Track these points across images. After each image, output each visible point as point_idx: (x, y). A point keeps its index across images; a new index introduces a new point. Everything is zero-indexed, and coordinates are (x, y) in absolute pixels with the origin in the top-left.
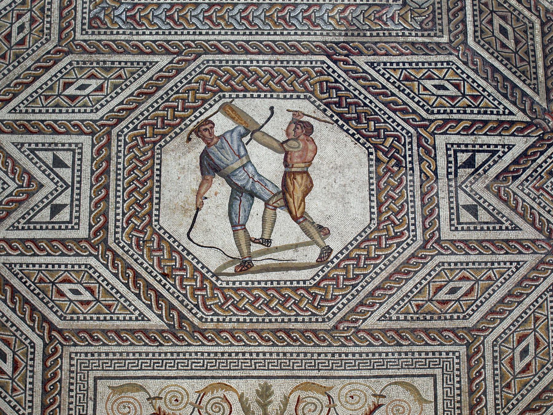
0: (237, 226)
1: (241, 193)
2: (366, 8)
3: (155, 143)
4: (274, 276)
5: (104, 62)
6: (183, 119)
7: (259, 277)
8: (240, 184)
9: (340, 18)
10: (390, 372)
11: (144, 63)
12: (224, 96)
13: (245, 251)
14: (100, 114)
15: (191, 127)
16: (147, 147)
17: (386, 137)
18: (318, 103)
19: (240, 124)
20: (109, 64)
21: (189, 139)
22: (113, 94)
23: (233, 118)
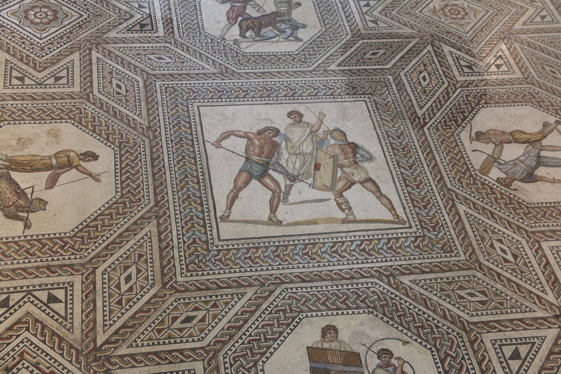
1: (540, 162)
2: (380, 111)
3: (527, 207)
5: (477, 241)
6: (502, 194)
8: (535, 163)
9: (392, 122)
11: (468, 218)
12: (476, 174)
14: (520, 239)
15: (506, 189)
16: (532, 211)
17: (468, 100)
18: (459, 130)
19: (492, 166)
20: (478, 238)
21: (515, 190)
22: (501, 233)
23: (490, 169)
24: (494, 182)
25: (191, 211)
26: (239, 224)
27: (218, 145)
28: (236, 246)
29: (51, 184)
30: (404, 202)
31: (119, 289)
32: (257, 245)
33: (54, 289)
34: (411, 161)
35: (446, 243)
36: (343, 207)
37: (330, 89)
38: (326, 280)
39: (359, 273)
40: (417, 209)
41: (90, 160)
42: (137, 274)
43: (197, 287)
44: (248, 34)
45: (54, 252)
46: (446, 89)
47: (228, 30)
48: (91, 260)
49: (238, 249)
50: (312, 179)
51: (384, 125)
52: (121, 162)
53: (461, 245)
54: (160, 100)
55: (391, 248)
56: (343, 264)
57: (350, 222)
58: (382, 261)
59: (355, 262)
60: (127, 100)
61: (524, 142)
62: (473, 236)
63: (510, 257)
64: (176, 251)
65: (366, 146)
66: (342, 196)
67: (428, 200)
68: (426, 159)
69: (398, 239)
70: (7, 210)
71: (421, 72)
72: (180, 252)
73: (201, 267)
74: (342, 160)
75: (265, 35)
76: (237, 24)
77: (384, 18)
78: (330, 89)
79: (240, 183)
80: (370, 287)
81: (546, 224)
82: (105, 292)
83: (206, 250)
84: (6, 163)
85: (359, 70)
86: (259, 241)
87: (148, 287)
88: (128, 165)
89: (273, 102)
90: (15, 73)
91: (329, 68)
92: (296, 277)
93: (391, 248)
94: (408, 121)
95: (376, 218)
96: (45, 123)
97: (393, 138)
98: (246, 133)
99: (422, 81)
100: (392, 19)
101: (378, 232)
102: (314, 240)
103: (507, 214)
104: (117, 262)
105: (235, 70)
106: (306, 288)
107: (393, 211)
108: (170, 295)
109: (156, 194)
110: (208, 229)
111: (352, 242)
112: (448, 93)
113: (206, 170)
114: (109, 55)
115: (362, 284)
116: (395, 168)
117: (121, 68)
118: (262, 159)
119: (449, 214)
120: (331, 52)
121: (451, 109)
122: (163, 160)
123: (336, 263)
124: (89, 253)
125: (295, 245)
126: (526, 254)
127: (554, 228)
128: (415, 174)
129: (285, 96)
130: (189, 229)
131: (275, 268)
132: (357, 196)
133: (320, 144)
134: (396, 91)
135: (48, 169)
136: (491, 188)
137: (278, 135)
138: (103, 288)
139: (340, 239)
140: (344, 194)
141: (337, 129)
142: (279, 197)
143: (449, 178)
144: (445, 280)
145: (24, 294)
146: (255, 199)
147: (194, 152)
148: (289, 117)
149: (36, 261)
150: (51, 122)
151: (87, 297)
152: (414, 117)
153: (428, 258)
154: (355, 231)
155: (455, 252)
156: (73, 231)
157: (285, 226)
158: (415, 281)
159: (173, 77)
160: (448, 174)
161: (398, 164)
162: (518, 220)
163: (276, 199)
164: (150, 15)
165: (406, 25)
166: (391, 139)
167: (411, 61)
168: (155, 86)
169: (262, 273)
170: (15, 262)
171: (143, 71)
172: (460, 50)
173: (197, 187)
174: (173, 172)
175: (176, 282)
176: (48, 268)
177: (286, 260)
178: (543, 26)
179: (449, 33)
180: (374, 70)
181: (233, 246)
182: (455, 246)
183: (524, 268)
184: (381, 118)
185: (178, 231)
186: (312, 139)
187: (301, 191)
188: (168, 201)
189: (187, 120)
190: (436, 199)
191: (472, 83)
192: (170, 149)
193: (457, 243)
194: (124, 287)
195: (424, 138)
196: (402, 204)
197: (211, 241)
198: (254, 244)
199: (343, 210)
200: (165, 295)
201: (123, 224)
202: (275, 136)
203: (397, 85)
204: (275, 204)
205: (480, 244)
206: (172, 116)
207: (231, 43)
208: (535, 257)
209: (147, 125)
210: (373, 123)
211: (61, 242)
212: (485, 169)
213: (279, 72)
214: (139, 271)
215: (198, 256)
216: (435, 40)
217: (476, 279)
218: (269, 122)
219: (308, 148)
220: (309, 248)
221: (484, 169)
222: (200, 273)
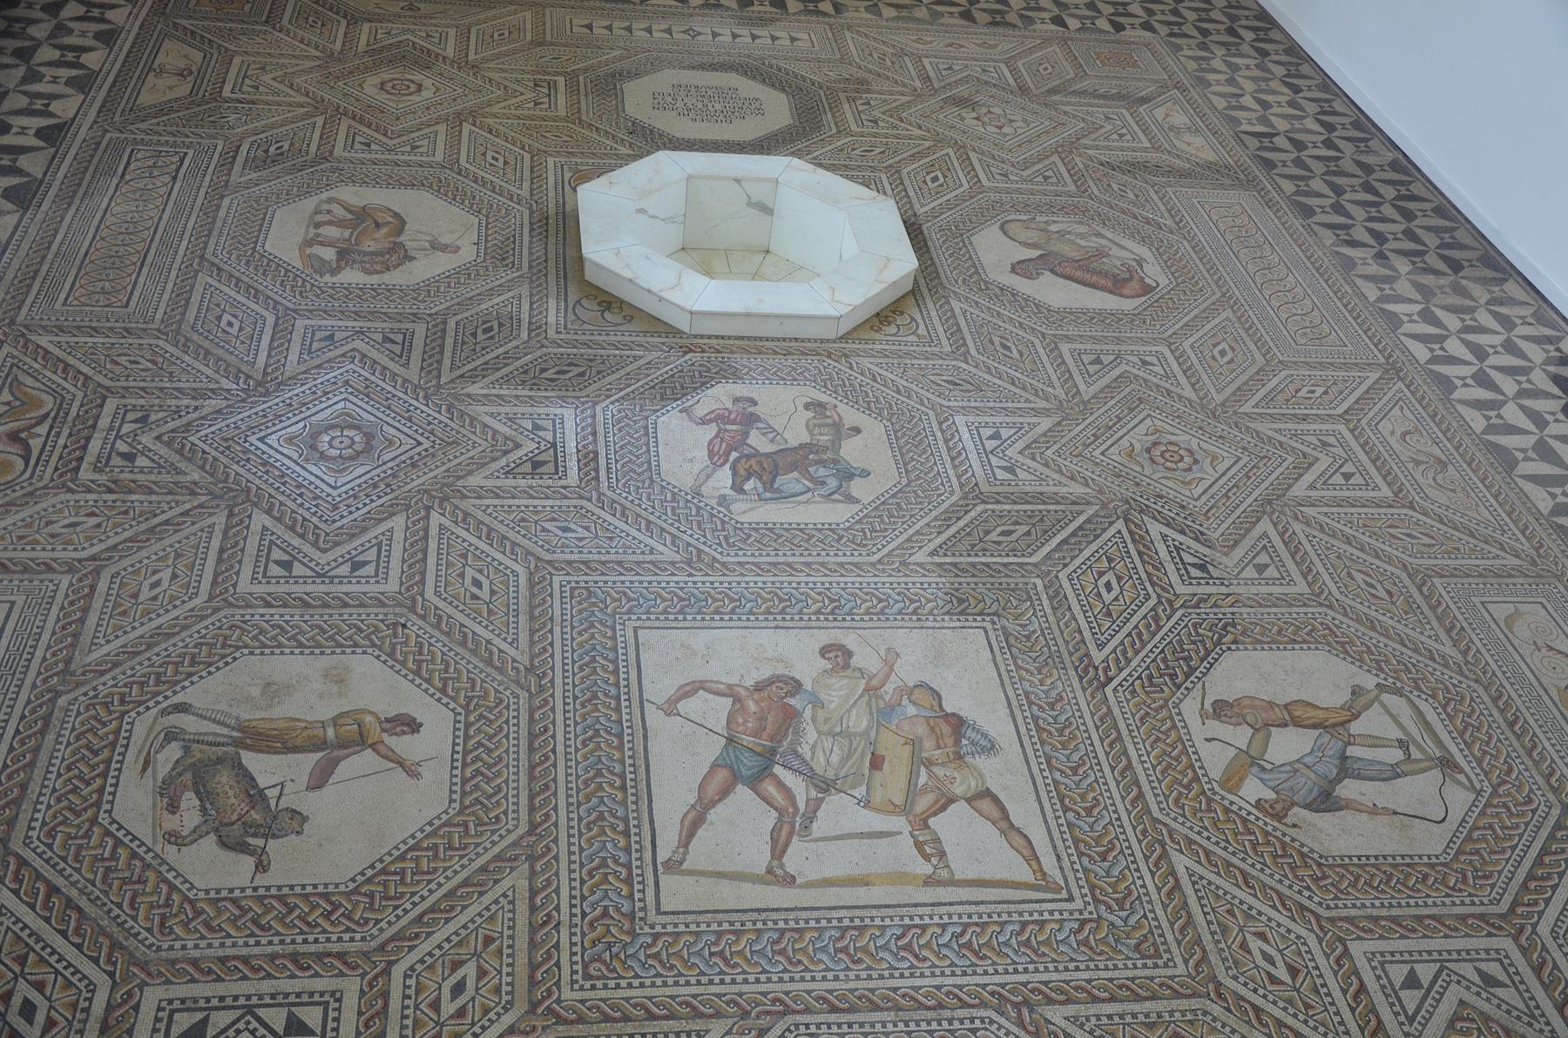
0: (1395, 773)
1: (1346, 768)
3: (1320, 865)
4: (1444, 736)
5: (1213, 934)
6: (1267, 834)
7: (1454, 750)
8: (1335, 771)
9: (1040, 673)
10: (1502, 637)
11: (1194, 883)
13: (1427, 764)
14: (1304, 933)
17: (1198, 634)
20: (1214, 927)
21: (1294, 826)
22: (1264, 918)
23: (1242, 780)
24: (1249, 808)
25: (604, 848)
26: (703, 880)
27: (670, 708)
28: (693, 928)
29: (320, 779)
30: (1059, 843)
31: (437, 1010)
32: (738, 926)
33: (302, 1004)
34: (1076, 757)
35: (1145, 936)
36: (929, 851)
37: (912, 601)
38: (882, 1009)
39: (956, 996)
40: (1085, 860)
41: (404, 733)
42: (479, 978)
43: (603, 1013)
44: (746, 487)
45: (309, 924)
46: (1152, 609)
47: (709, 476)
48: (382, 947)
49: (697, 934)
50: (864, 788)
51: (1021, 679)
52: (467, 737)
53: (1179, 943)
54: (557, 612)
55: (1027, 944)
56: (922, 975)
57: (940, 883)
58: (1007, 972)
59: (948, 971)
60: (490, 612)
61: (1314, 726)
62: (1204, 923)
63: (1282, 973)
64: (564, 932)
65: (982, 723)
66: (927, 827)
67: (1110, 842)
68: (1107, 754)
69: (1042, 924)
70: (224, 831)
71: (1101, 574)
72: (572, 934)
73: (614, 970)
74: (929, 749)
75: (784, 488)
76: (728, 466)
77: (1029, 462)
78: (912, 601)
79: (711, 790)
80: (978, 1029)
81: (1358, 903)
82: (407, 1017)
83: (628, 933)
84: (235, 734)
85: (973, 565)
86: (743, 917)
87: (499, 1009)
88: (480, 744)
89: (791, 624)
90: (277, 554)
91: (912, 559)
92: (817, 999)
93: (1027, 944)
94: (1072, 673)
95: (998, 877)
96: (322, 653)
97: (1040, 707)
98: (730, 687)
99: (1103, 591)
100: (1046, 465)
101: (1000, 907)
102: (862, 920)
103: (1277, 877)
104: (437, 952)
105: (718, 556)
106: (839, 1025)
107: (1033, 863)
108: (544, 1028)
109: (532, 810)
110: (637, 887)
111: (944, 927)
112: (1156, 618)
113: (641, 763)
114: (464, 520)
115: (961, 1021)
116: (1042, 771)
117: (486, 548)
118: (762, 743)
119: (1153, 874)
120: (917, 527)
121: (1162, 651)
122: (553, 737)
123: (907, 973)
124: (381, 930)
125: (821, 930)
126: (1317, 968)
127: (1375, 912)
128: (1085, 784)
129: (818, 612)
130: (597, 886)
131: (775, 978)
132: (960, 830)
133: (884, 714)
134: (1048, 610)
135: (317, 749)
136: (1244, 821)
137: (797, 692)
138: (405, 1007)
139: (917, 921)
140: (931, 821)
141: (921, 685)
142: (793, 825)
143: (1156, 795)
144: (1141, 1018)
145: (239, 1013)
146: (742, 826)
147: (620, 722)
148: (823, 656)
149: (270, 943)
150: (333, 653)
151: (367, 1026)
152: (1085, 666)
153: (1107, 969)
154: (951, 904)
155: (1166, 956)
156: (353, 880)
157: (801, 886)
158: (1076, 1018)
159: (588, 567)
160: (1153, 788)
161: (1049, 762)
162: (1300, 892)
163: (786, 828)
164: (554, 445)
165: (1072, 479)
166: (1035, 708)
167: (1081, 551)
168: (551, 584)
169: (745, 988)
170: (229, 942)
171: (529, 553)
172: (1182, 532)
173: (620, 796)
174: (573, 763)
175: (558, 1001)
176: (294, 958)
177: (800, 962)
178: (1348, 493)
179: (1162, 497)
180: (1005, 565)
181: (687, 926)
182: (1165, 943)
183: (1313, 999)
184: (1016, 664)
185: (571, 888)
186: (869, 704)
187: (840, 812)
188: (556, 824)
189: (611, 656)
190: (1127, 840)
191: (1206, 601)
192: (571, 715)
193: (1170, 937)
194: (448, 1008)
195: (1105, 709)
196: (1055, 847)
197: (641, 914)
198: (732, 924)
199: (927, 858)
200: (534, 1028)
201: (457, 871)
202: (793, 695)
203: (1051, 599)
204: (782, 840)
205: (1219, 942)
206: (581, 645)
207: (713, 502)
208: (1335, 973)
209: (527, 663)
210: (1000, 675)
211: (326, 904)
212: (1232, 780)
213: (808, 564)
214: (482, 973)
215: (610, 946)
216: (1132, 512)
217: (1208, 1019)
218: (779, 665)
219: (859, 721)
220: (851, 936)
221: (1229, 779)
222: (612, 984)
